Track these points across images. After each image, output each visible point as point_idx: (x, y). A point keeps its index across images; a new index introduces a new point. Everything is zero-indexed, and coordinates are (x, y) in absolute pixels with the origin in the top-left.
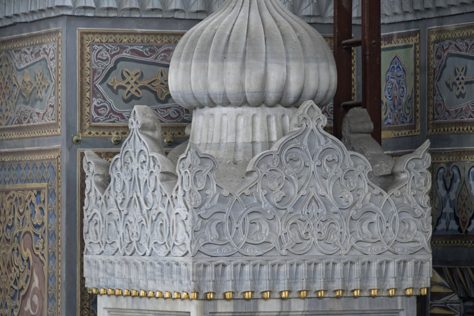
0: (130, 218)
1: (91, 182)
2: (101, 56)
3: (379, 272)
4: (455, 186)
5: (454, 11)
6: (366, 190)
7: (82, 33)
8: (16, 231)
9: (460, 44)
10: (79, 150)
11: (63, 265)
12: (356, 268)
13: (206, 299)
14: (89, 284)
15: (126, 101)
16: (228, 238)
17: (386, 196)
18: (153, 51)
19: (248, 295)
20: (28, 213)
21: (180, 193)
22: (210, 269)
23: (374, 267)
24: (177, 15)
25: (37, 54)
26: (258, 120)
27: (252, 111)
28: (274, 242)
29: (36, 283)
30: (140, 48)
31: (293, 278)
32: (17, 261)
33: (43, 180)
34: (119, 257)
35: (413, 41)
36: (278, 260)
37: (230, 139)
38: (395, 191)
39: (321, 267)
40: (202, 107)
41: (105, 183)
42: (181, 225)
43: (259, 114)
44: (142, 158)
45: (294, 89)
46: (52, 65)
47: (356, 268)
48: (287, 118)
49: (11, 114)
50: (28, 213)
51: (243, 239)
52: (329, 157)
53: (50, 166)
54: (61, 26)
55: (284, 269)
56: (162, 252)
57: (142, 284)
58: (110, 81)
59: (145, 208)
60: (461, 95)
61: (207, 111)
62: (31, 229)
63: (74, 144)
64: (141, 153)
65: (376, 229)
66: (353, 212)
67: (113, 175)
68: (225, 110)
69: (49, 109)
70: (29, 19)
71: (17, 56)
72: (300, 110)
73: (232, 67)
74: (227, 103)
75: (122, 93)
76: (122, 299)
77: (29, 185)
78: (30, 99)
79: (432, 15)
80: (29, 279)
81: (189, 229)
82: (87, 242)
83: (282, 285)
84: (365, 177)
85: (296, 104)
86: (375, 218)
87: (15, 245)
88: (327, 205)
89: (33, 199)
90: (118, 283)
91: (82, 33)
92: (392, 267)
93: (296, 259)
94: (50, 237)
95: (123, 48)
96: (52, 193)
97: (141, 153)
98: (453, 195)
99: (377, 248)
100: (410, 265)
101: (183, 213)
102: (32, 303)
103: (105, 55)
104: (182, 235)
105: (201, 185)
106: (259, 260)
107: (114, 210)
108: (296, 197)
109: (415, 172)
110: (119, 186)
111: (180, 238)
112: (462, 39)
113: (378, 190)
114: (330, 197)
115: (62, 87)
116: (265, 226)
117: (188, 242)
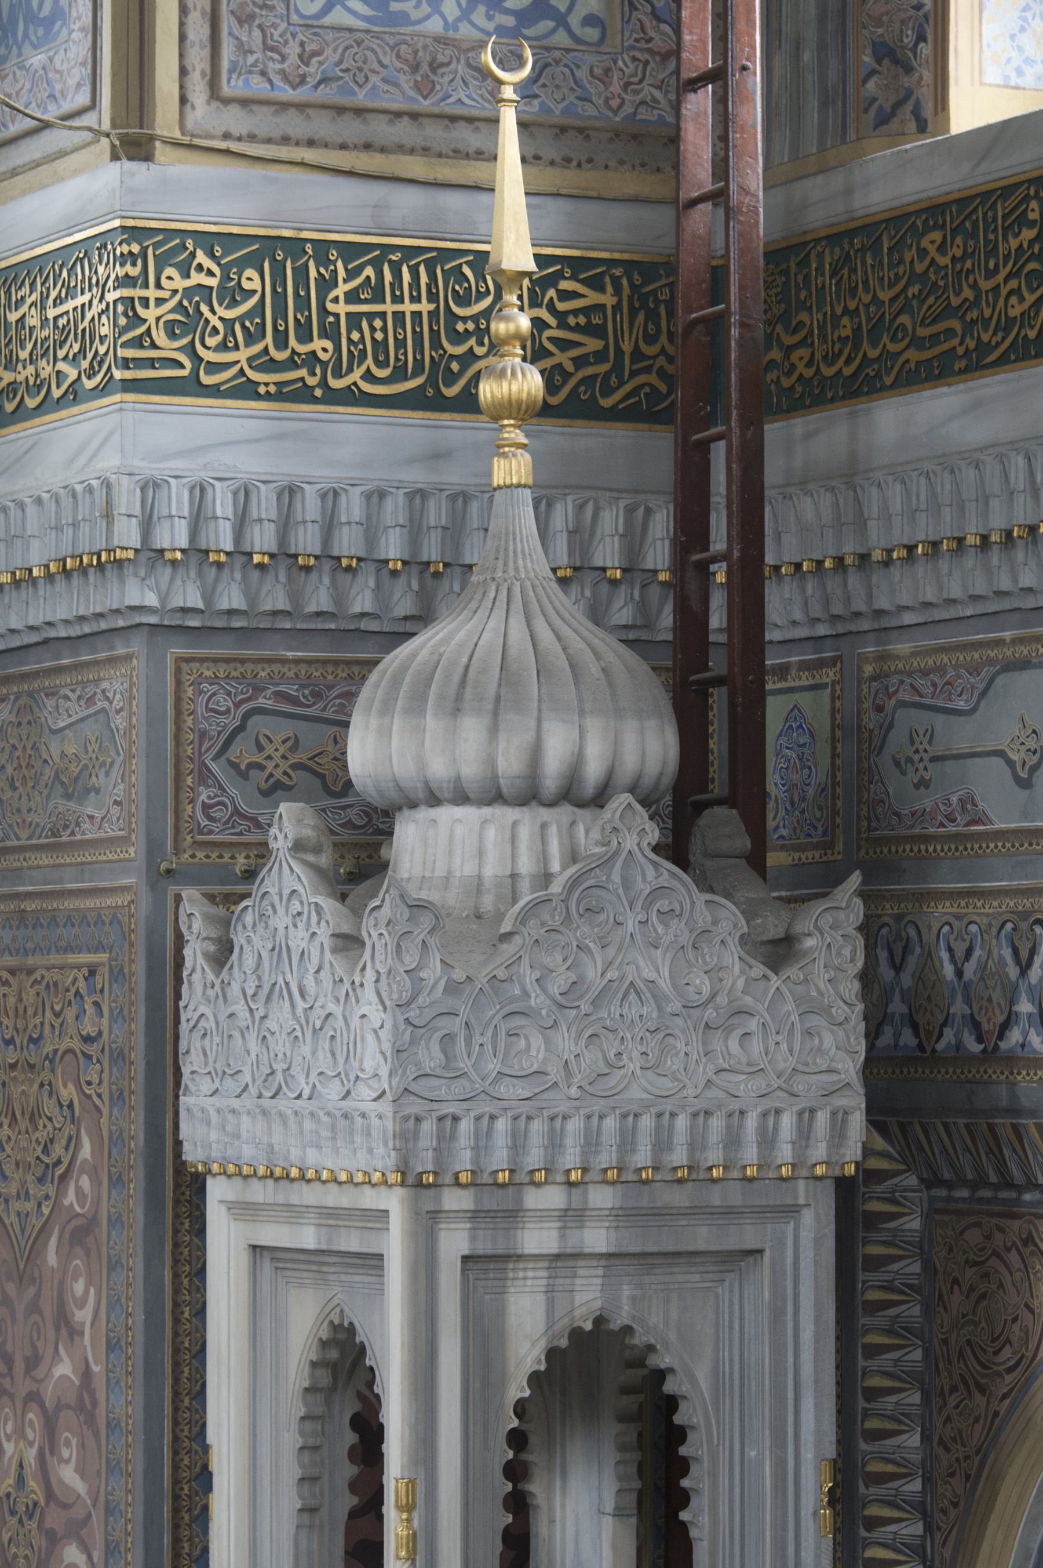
0: (272, 1024)
1: (194, 954)
2: (215, 704)
3: (762, 1130)
4: (912, 961)
5: (909, 619)
6: (736, 969)
7: (180, 660)
8: (48, 1049)
9: (920, 682)
10: (172, 889)
11: (139, 1117)
12: (717, 1123)
13: (420, 1185)
14: (192, 1154)
15: (266, 793)
16: (464, 1064)
17: (775, 981)
18: (317, 695)
19: (503, 1177)
20: (70, 1014)
21: (370, 975)
22: (428, 1126)
23: (751, 1122)
24: (365, 625)
25: (90, 701)
26: (525, 833)
27: (508, 814)
28: (555, 1072)
29: (86, 1151)
30: (292, 690)
31: (591, 1143)
32: (49, 1106)
33: (99, 948)
34: (248, 1102)
35: (828, 676)
36: (563, 1107)
37: (469, 869)
38: (793, 972)
39: (646, 1122)
40: (413, 805)
41: (223, 953)
42: (370, 1038)
43: (526, 821)
44: (296, 906)
45: (594, 771)
46: (119, 721)
47: (717, 1123)
48: (581, 829)
49: (39, 818)
50: (70, 1014)
51: (492, 1066)
52: (663, 904)
53: (115, 920)
54: (137, 645)
55: (574, 1125)
56: (333, 1091)
57: (295, 1154)
58: (232, 754)
59: (301, 1005)
60: (924, 783)
61: (424, 813)
62: (76, 1044)
63: (163, 877)
64: (291, 897)
65: (756, 1046)
66: (710, 1013)
67: (239, 939)
68: (459, 811)
69: (115, 808)
70: (74, 631)
71: (50, 703)
72: (607, 814)
73: (472, 729)
74: (461, 798)
75: (258, 778)
76: (255, 1183)
77: (72, 958)
78: (76, 786)
79: (865, 625)
80: (73, 1143)
81: (387, 1046)
82: (186, 1070)
83: (571, 1158)
84: (733, 943)
85: (599, 800)
86: (753, 1025)
87: (46, 1076)
88: (659, 998)
89: (81, 984)
90: (248, 1152)
91: (180, 660)
92: (787, 1121)
93: (597, 1106)
94: (114, 1061)
95: (258, 690)
96: (118, 974)
97: (291, 897)
98: (907, 980)
99: (758, 1084)
100: (822, 1118)
101: (376, 1015)
102: (79, 1190)
103: (223, 702)
104: (373, 1058)
105: (410, 960)
106: (525, 1108)
107: (240, 1008)
108: (599, 984)
109: (833, 934)
110: (249, 962)
111: (369, 1065)
112: (925, 673)
113: (759, 969)
114: (665, 984)
115: (138, 765)
116: (537, 1042)
117: (384, 1072)
